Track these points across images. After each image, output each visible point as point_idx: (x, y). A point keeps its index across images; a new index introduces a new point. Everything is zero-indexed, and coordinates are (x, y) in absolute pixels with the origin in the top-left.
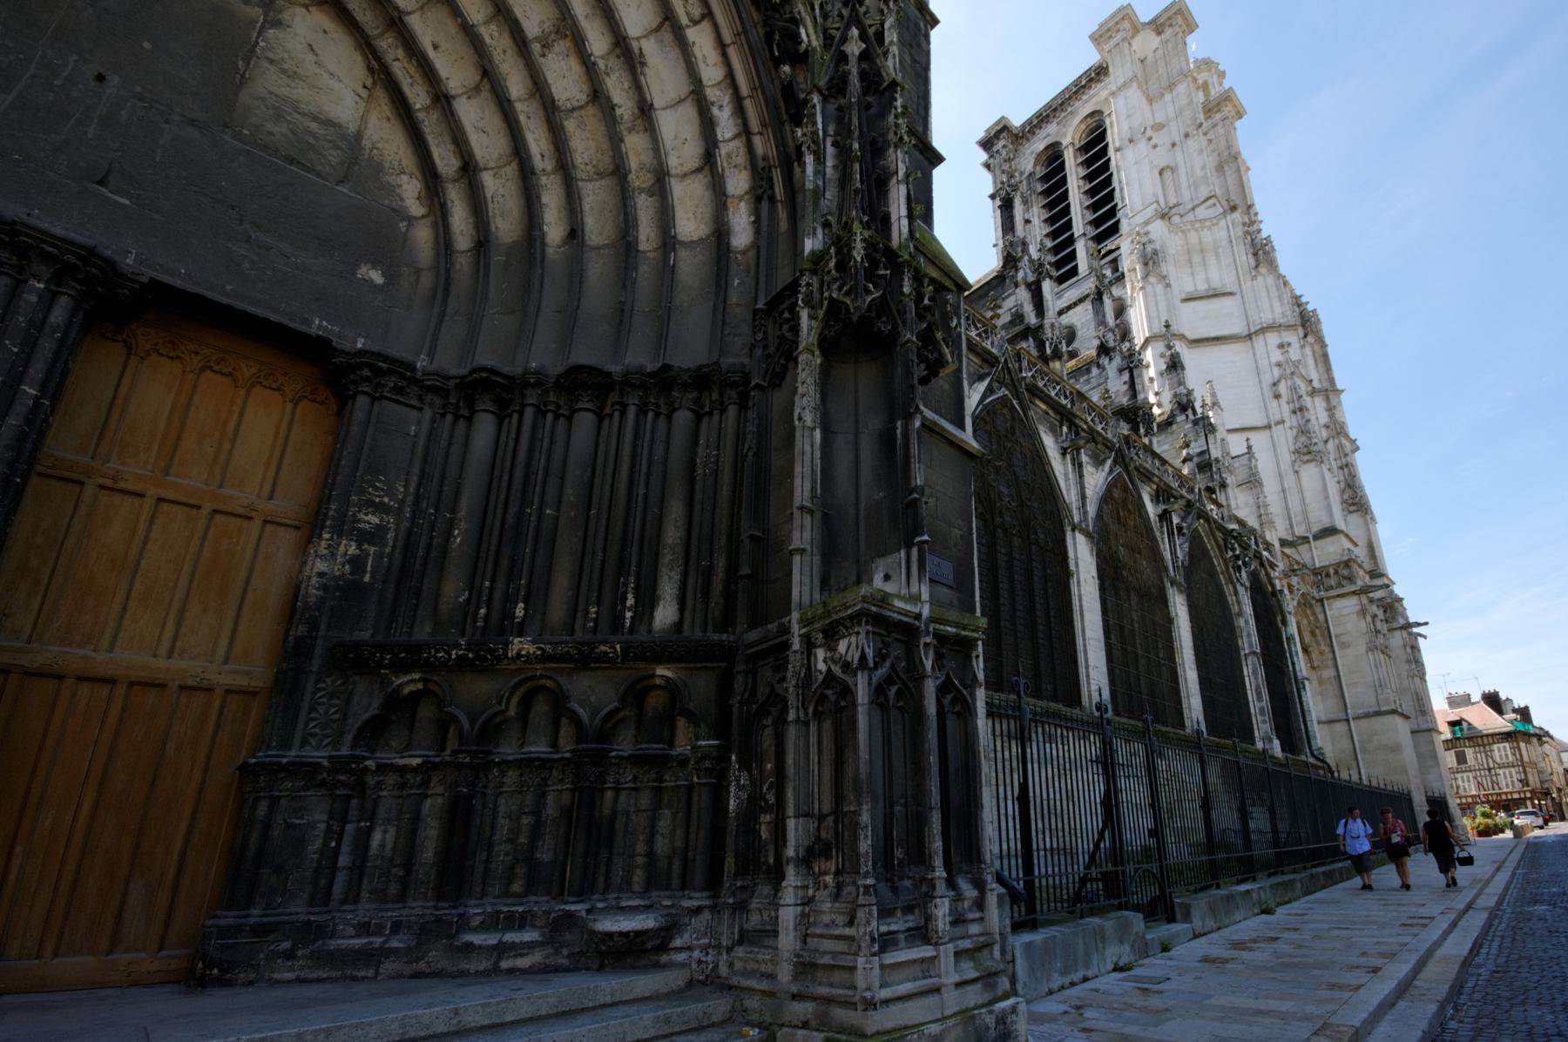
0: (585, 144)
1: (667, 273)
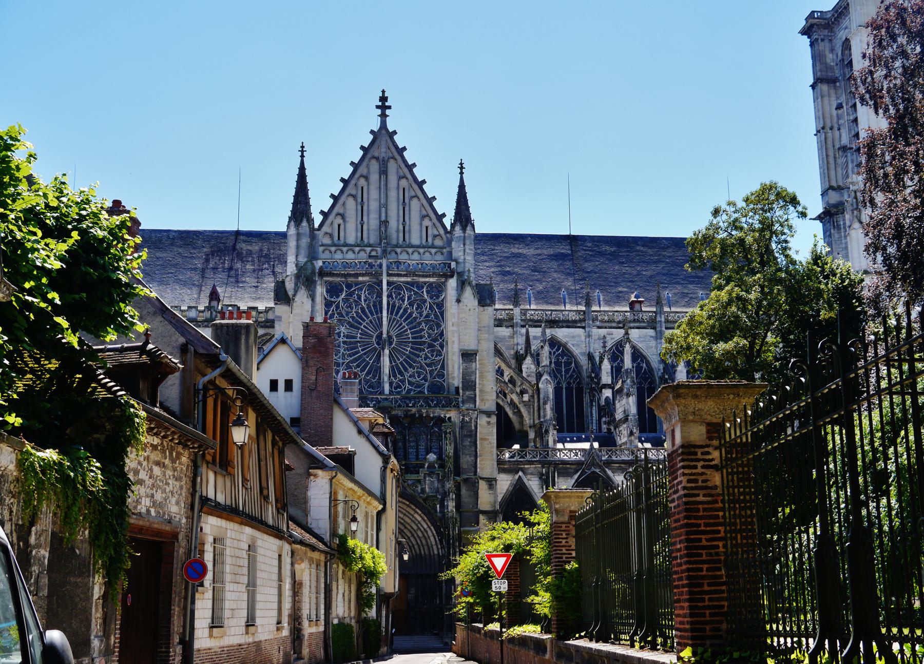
0: (424, 542)
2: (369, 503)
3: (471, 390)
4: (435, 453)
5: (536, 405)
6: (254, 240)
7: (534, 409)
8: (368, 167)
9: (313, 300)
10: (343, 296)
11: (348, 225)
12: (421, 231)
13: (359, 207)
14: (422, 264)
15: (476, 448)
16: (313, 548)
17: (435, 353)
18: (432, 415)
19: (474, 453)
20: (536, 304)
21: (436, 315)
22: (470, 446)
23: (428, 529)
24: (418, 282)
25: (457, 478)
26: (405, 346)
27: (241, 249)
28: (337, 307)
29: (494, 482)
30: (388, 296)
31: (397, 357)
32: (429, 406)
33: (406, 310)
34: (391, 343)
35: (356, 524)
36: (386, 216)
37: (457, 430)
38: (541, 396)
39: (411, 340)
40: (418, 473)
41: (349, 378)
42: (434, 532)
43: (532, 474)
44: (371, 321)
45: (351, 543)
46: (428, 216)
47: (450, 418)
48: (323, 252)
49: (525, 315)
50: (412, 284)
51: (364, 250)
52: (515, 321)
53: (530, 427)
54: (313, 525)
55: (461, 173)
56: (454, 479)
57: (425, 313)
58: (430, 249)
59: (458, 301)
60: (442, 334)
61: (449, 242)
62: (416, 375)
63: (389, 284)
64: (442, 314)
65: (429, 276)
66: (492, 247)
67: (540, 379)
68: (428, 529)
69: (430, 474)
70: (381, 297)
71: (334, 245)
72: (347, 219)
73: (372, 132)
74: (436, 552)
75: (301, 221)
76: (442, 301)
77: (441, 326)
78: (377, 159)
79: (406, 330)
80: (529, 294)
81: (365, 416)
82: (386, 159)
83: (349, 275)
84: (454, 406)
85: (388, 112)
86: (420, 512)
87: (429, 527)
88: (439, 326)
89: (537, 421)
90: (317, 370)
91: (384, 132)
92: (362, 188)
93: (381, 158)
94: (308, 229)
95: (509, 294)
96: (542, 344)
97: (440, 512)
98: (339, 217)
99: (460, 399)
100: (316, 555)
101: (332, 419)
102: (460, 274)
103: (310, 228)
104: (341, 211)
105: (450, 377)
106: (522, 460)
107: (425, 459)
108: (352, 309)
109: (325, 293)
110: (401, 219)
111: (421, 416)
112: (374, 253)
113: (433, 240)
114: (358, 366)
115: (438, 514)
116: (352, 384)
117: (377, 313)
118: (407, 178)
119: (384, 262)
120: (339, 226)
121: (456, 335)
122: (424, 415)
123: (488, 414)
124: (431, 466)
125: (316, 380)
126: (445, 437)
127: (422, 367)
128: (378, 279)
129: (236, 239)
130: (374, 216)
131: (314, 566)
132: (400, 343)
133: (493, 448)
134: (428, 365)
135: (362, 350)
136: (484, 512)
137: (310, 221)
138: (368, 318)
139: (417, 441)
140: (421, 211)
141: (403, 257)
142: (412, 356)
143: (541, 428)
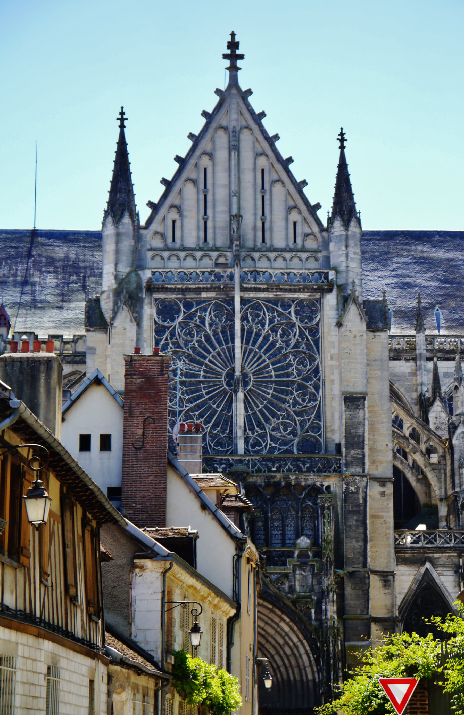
0: (293, 662)
1: (308, 687)
2: (216, 606)
3: (359, 449)
4: (308, 536)
5: (449, 468)
6: (58, 242)
7: (445, 474)
8: (213, 140)
9: (139, 324)
10: (180, 319)
11: (186, 221)
12: (287, 228)
13: (202, 197)
14: (288, 274)
15: (366, 529)
16: (139, 671)
17: (307, 397)
18: (303, 484)
19: (363, 536)
20: (448, 328)
21: (308, 345)
22: (357, 527)
23: (299, 644)
24: (283, 299)
25: (340, 571)
26: (265, 387)
27: (40, 255)
28: (172, 335)
29: (391, 578)
30: (244, 318)
31: (255, 403)
32: (300, 471)
33: (266, 338)
34: (246, 384)
35: (198, 635)
36: (239, 208)
37: (339, 503)
38: (456, 456)
39: (274, 379)
40: (284, 564)
41: (189, 432)
42: (308, 648)
43: (444, 566)
44: (219, 354)
45: (191, 663)
46: (296, 207)
47: (328, 488)
48: (153, 258)
49: (432, 343)
50: (275, 302)
51: (209, 256)
52: (418, 352)
53: (441, 500)
54: (138, 638)
55: (342, 148)
56: (335, 572)
57: (293, 342)
58: (299, 254)
59: (339, 324)
60: (316, 371)
61: (326, 244)
62: (281, 427)
63: (243, 301)
64: (317, 342)
65: (299, 291)
66: (386, 250)
67: (454, 432)
68: (299, 644)
69: (302, 566)
70: (233, 320)
71: (167, 249)
72: (185, 213)
73: (218, 92)
74: (310, 677)
75: (122, 216)
76: (317, 324)
77: (315, 360)
78: (226, 129)
79: (267, 366)
80: (437, 315)
81: (212, 484)
82: (238, 129)
83: (188, 290)
84: (335, 471)
85: (239, 63)
86: (288, 620)
87: (300, 640)
88: (312, 359)
89: (450, 492)
90: (144, 421)
91: (234, 91)
92: (205, 169)
93: (231, 129)
94: (131, 228)
95: (410, 315)
96: (456, 384)
97: (316, 620)
98: (174, 210)
99: (343, 461)
100: (142, 681)
101: (165, 489)
102: (341, 288)
103: (134, 226)
104: (177, 202)
105: (328, 430)
106: (429, 546)
107: (295, 544)
108: (192, 337)
109: (155, 315)
110: (260, 212)
111: (288, 484)
112: (222, 260)
113: (304, 240)
114: (201, 416)
115: (314, 623)
116: (193, 440)
117: (227, 343)
118: (267, 156)
119: (237, 272)
120: (174, 222)
121: (336, 372)
122: (293, 483)
123: (382, 481)
124: (303, 554)
125: (143, 434)
126: (323, 514)
127: (289, 416)
128: (228, 295)
129: (32, 243)
130: (222, 208)
131: (139, 696)
132: (258, 384)
133: (388, 528)
134: (298, 414)
135: (207, 393)
136: (377, 620)
137: (134, 216)
138: (214, 348)
139: (283, 520)
140: (286, 200)
141: (262, 265)
142: (275, 401)
143: (456, 501)
